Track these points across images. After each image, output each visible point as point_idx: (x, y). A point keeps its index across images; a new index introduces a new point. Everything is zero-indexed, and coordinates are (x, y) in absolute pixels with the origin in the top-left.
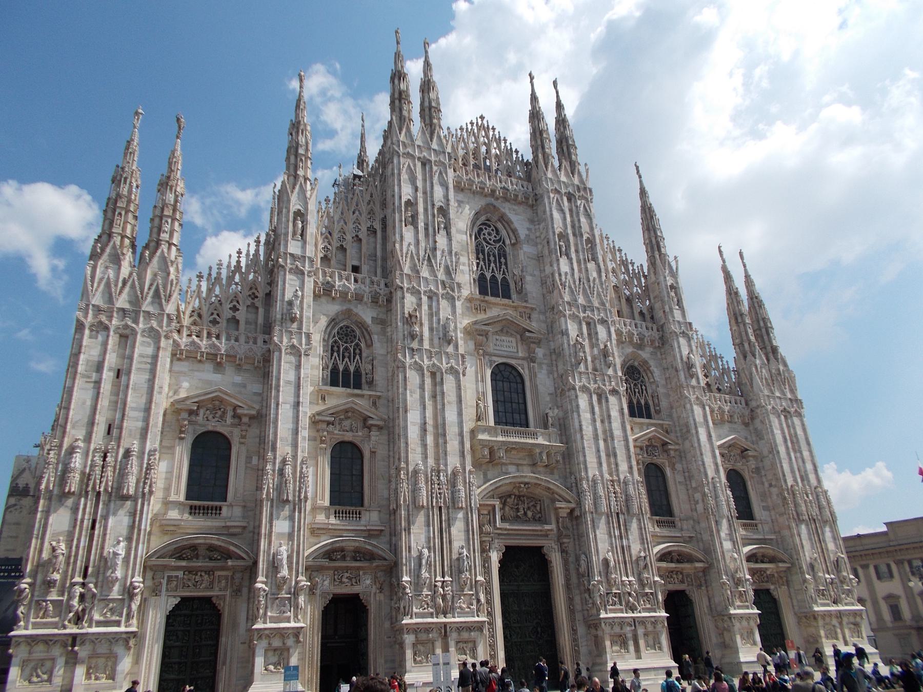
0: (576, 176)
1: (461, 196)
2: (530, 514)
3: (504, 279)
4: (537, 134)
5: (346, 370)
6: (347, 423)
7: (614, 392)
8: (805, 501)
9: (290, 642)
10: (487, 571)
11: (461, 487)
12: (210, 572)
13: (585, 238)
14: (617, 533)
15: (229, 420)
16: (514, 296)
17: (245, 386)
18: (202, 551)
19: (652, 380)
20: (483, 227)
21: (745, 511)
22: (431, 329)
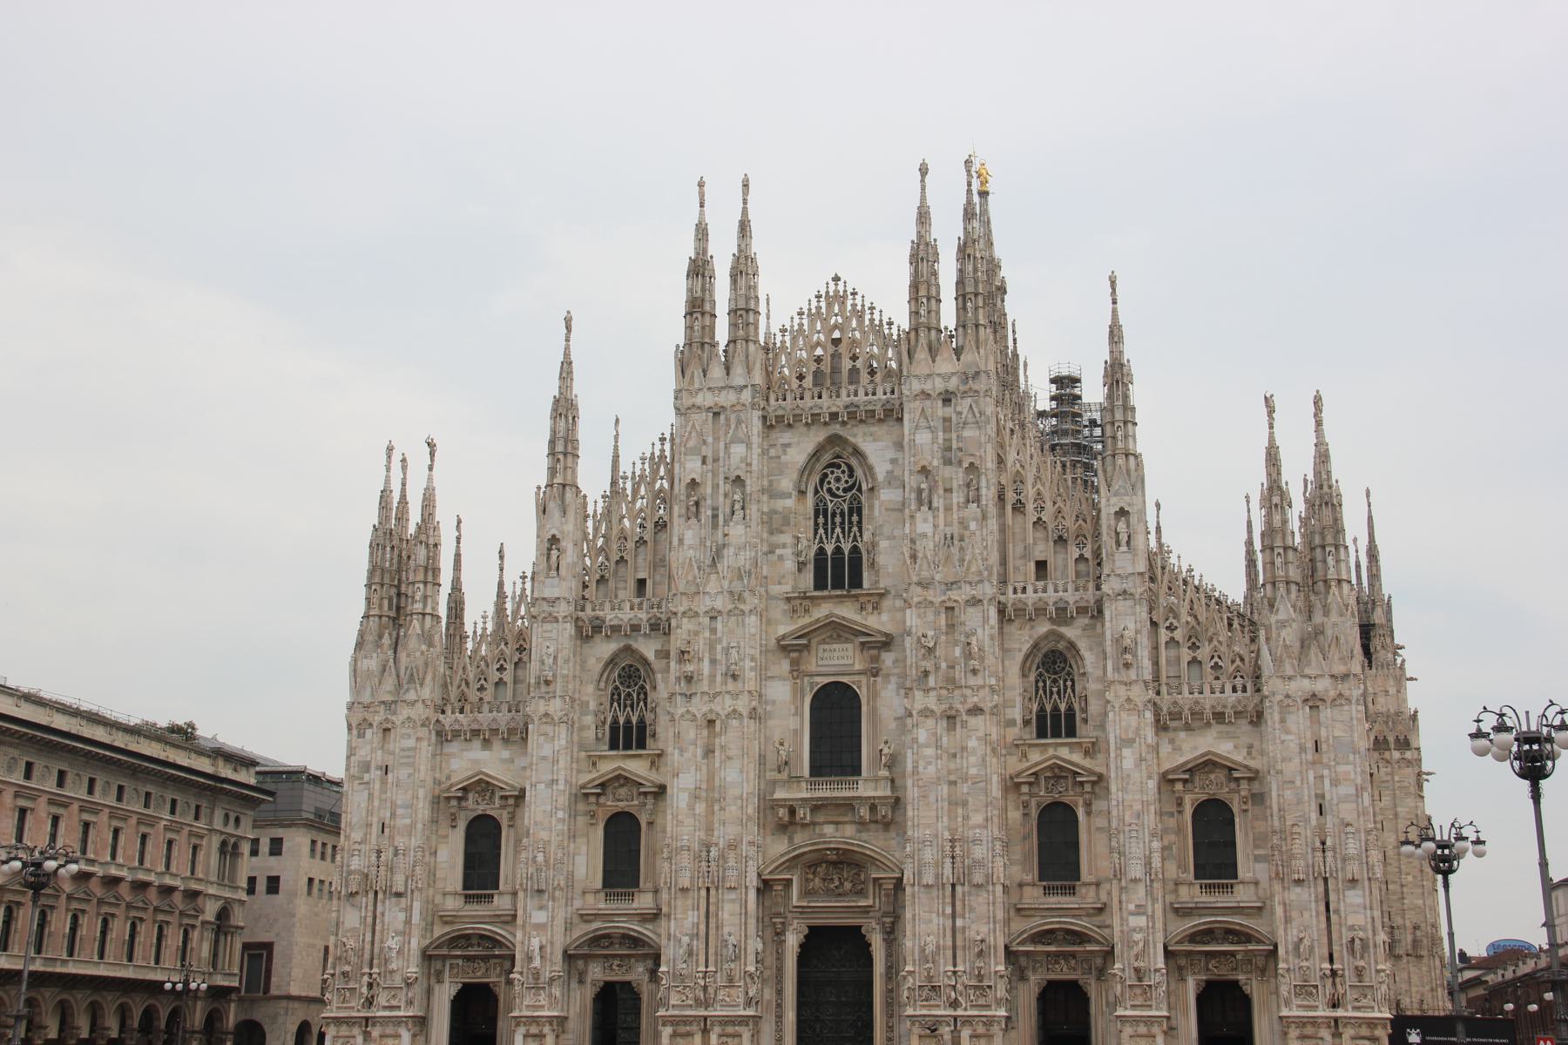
1: (786, 437)
2: (848, 885)
3: (855, 550)
4: (922, 289)
5: (628, 721)
6: (623, 791)
7: (976, 711)
8: (1314, 850)
9: (546, 1030)
10: (780, 957)
11: (732, 863)
12: (485, 959)
13: (966, 465)
14: (949, 910)
15: (497, 800)
16: (865, 575)
17: (512, 761)
18: (474, 941)
20: (828, 471)
22: (713, 662)
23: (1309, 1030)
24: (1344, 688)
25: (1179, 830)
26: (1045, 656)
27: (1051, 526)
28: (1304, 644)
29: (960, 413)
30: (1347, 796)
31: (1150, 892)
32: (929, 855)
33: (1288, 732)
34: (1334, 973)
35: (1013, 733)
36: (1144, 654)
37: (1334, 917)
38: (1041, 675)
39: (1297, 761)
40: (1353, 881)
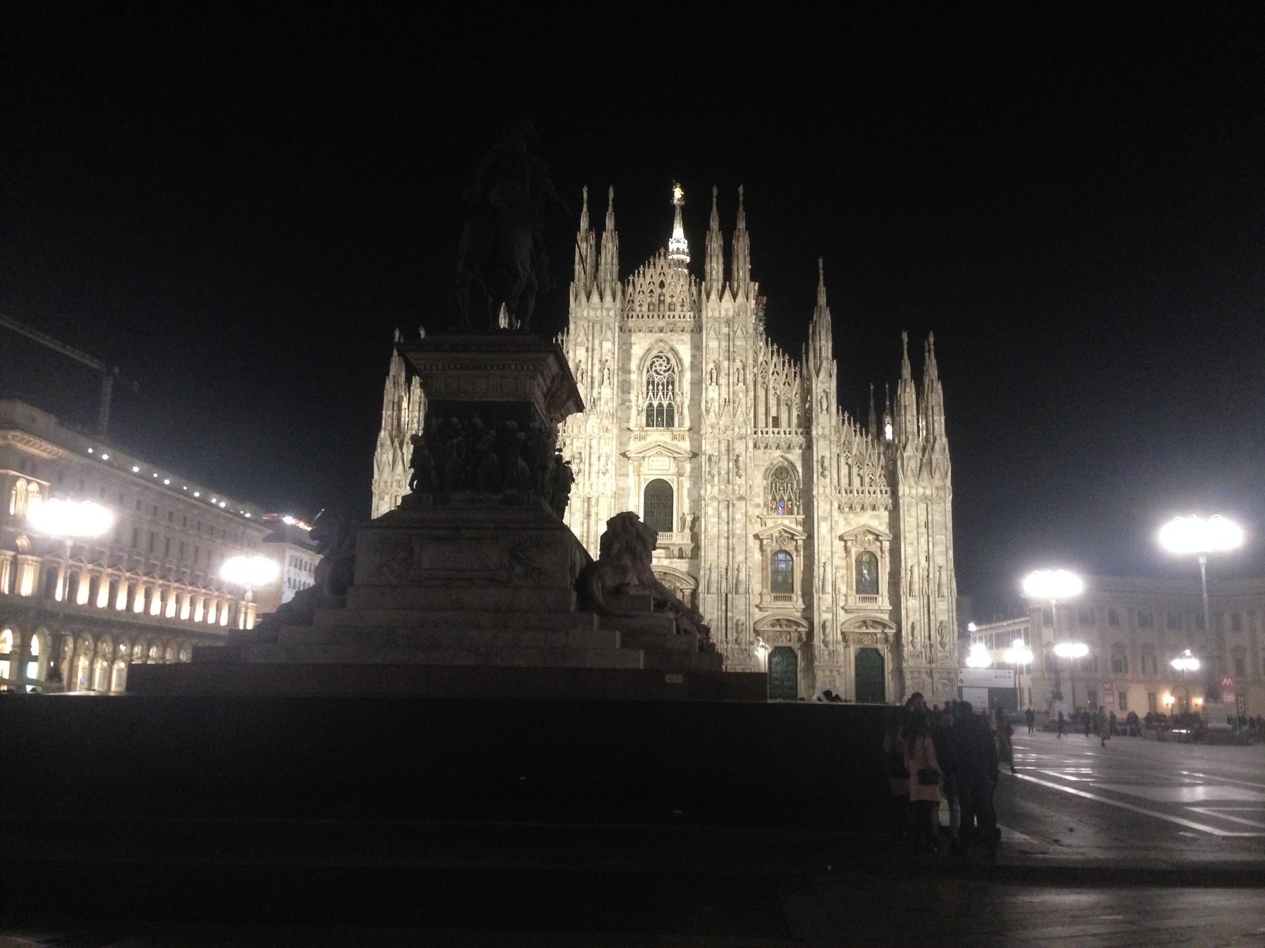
0: (740, 299)
3: (670, 405)
7: (741, 498)
21: (867, 587)
23: (916, 674)
24: (941, 493)
25: (848, 567)
27: (782, 397)
29: (735, 332)
31: (835, 601)
32: (714, 576)
33: (911, 516)
34: (931, 646)
35: (757, 512)
36: (834, 471)
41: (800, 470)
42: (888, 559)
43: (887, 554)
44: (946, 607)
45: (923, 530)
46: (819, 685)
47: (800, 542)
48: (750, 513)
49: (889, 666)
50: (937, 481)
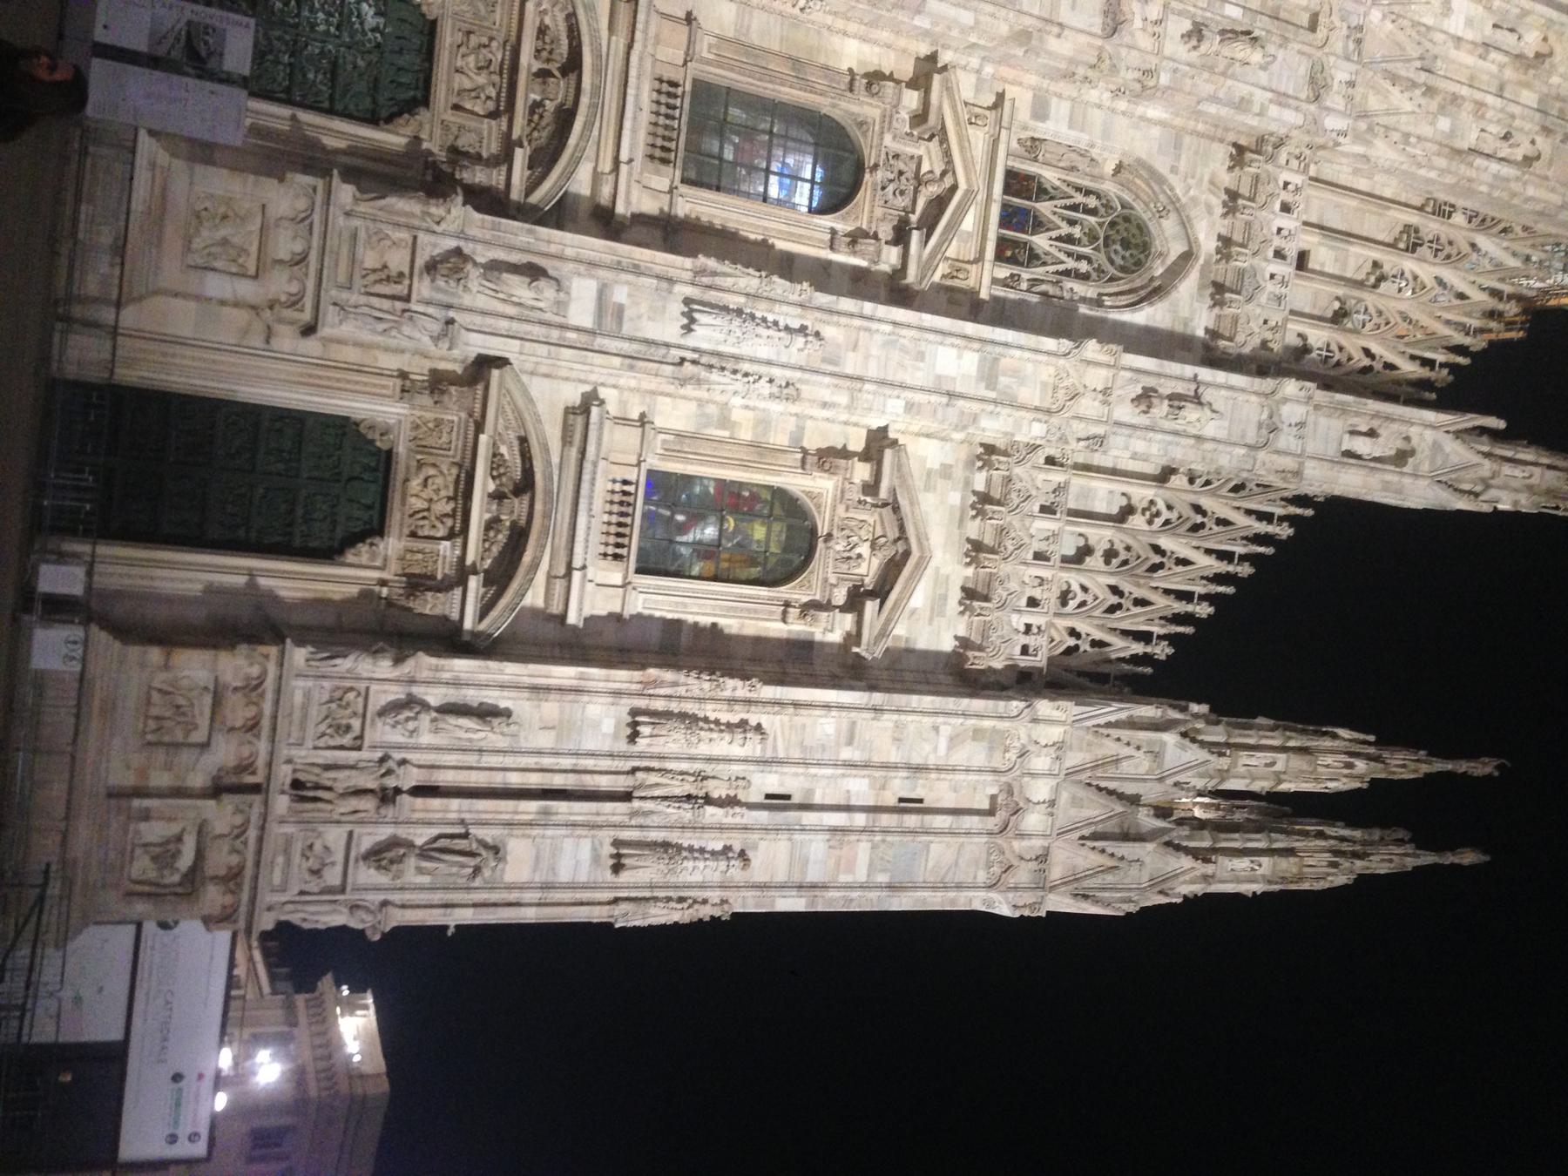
8: (702, 777)
19: (1108, 302)
23: (238, 712)
24: (1023, 875)
25: (761, 451)
26: (1142, 228)
27: (1370, 299)
28: (1111, 793)
30: (805, 862)
31: (646, 353)
33: (954, 741)
34: (387, 796)
35: (1021, 99)
37: (533, 806)
38: (1108, 206)
39: (894, 757)
40: (617, 868)
41: (1140, 317)
42: (775, 628)
43: (796, 628)
44: (564, 876)
45: (899, 786)
46: (219, 183)
47: (892, 256)
48: (1053, 44)
49: (291, 581)
50: (1069, 858)
